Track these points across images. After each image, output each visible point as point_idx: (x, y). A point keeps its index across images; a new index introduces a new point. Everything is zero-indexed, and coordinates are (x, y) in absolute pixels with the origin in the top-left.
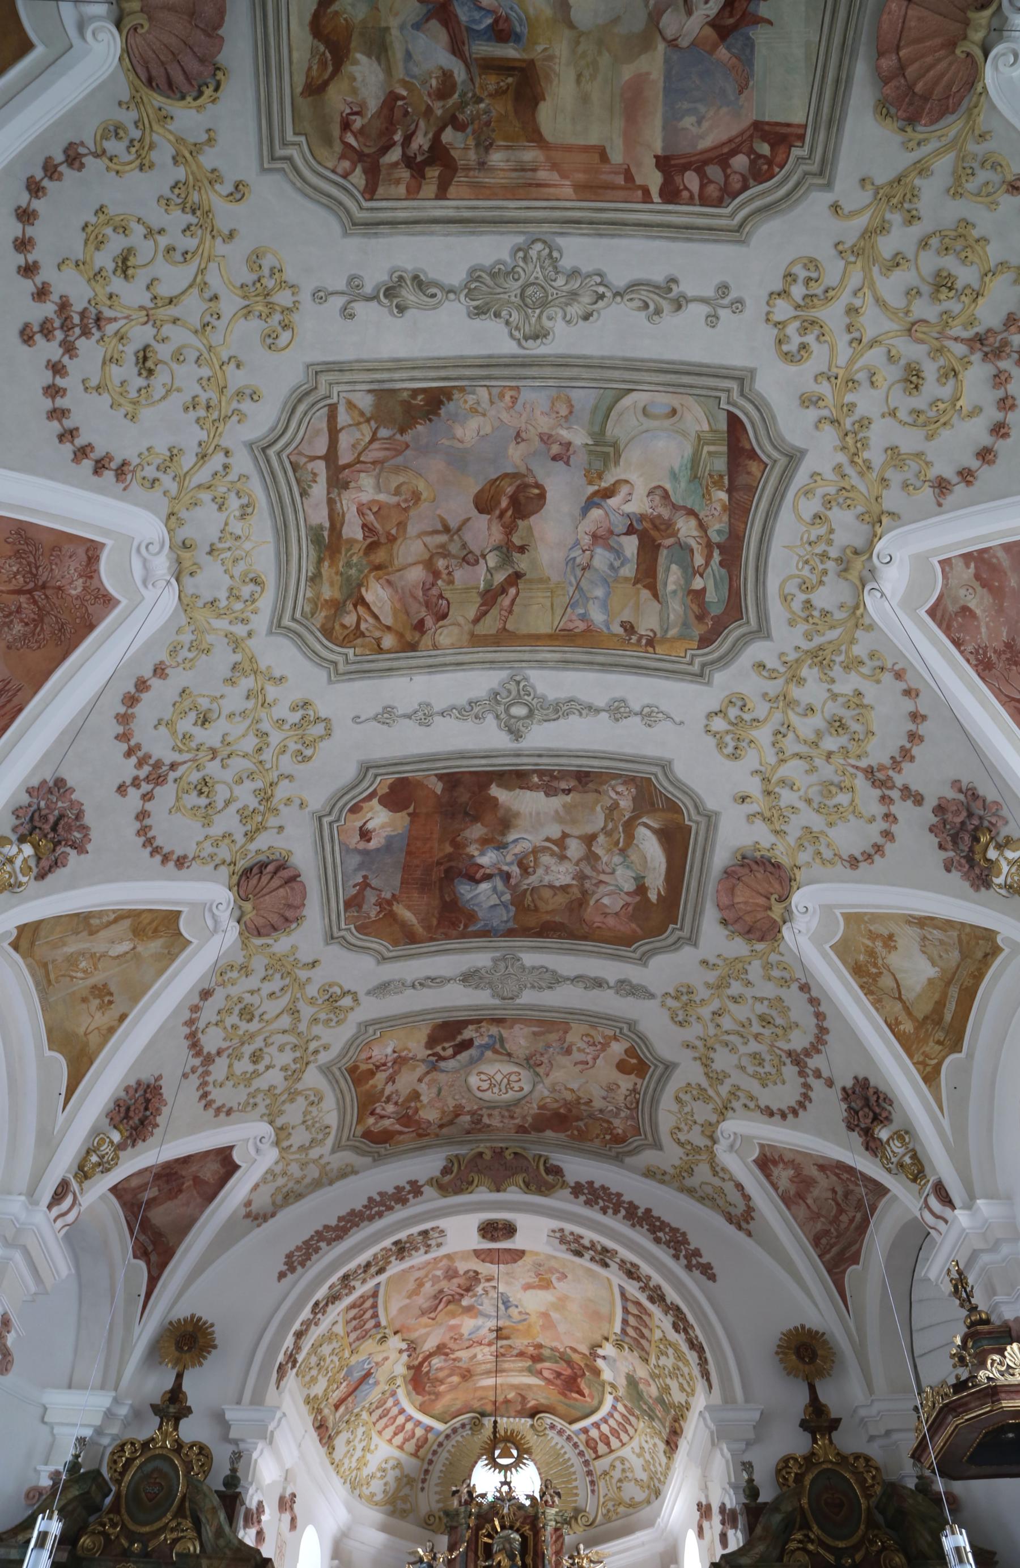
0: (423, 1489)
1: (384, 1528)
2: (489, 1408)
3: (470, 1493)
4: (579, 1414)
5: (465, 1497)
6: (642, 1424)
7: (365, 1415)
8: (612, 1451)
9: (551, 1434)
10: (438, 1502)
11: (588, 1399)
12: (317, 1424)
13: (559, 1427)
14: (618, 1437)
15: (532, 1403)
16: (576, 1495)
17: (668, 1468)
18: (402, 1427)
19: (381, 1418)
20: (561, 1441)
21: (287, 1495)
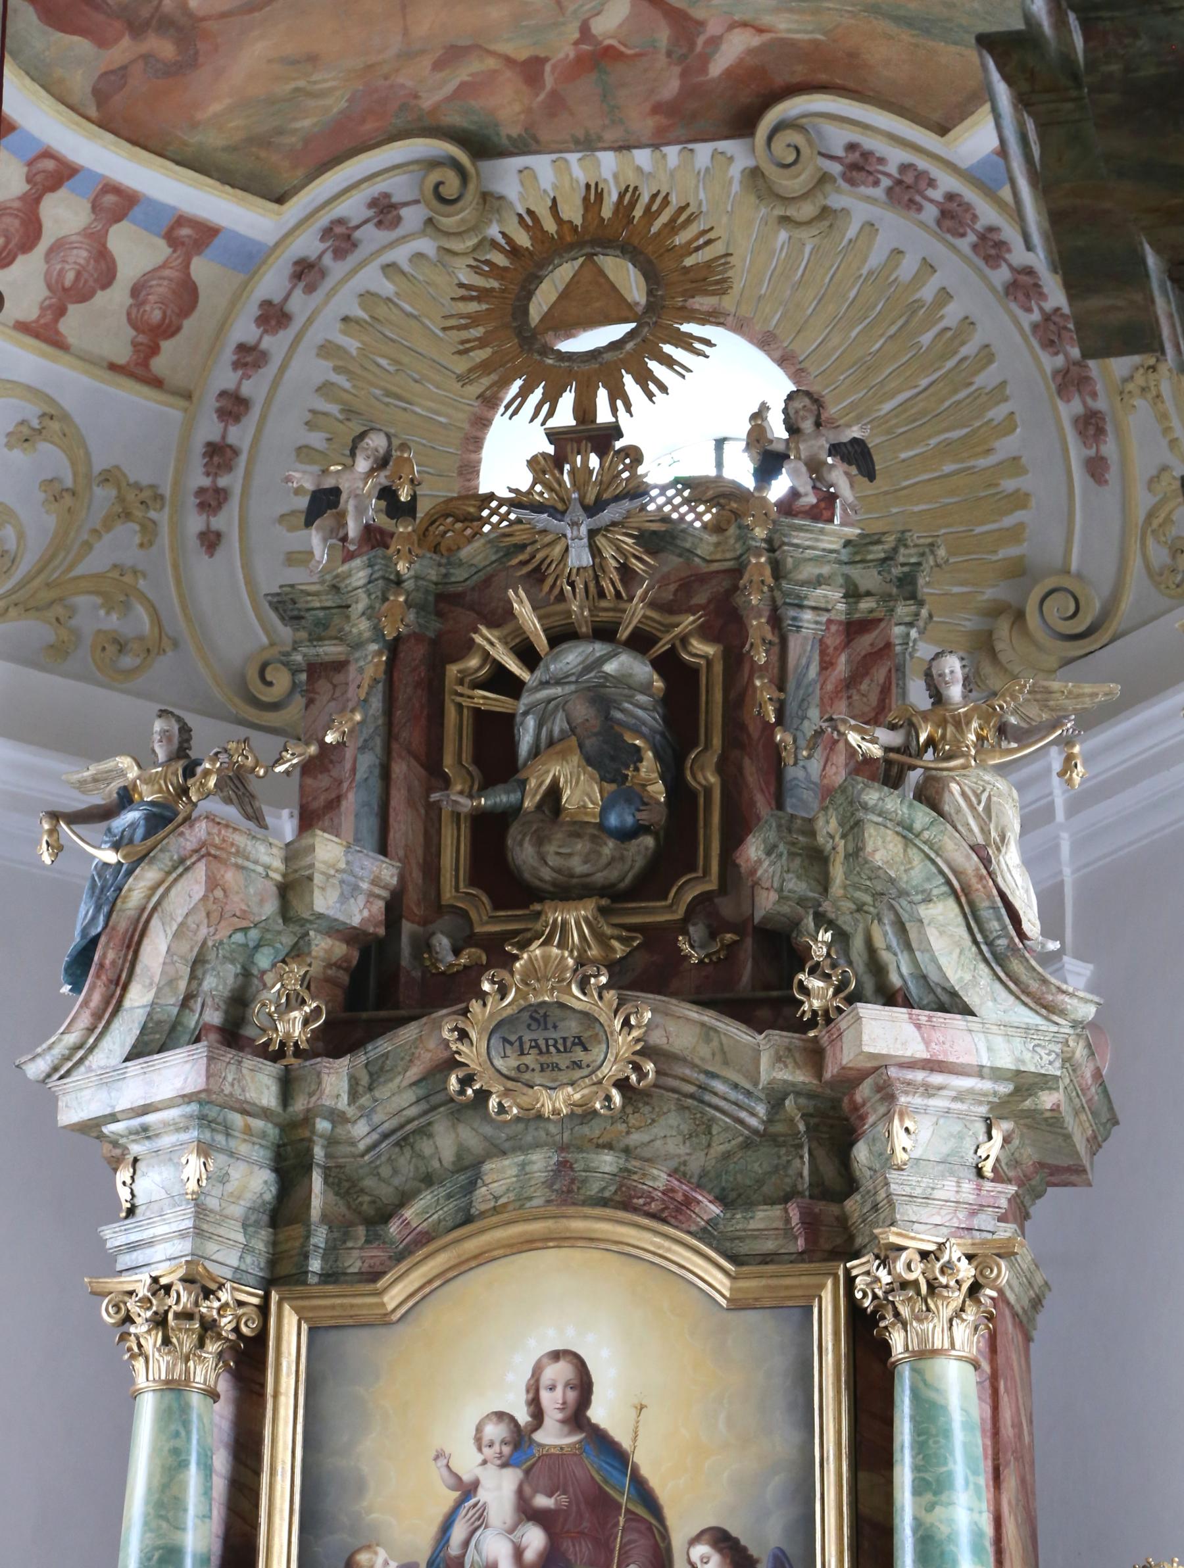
0: (211, 541)
13: (896, 157)
16: (1019, 500)
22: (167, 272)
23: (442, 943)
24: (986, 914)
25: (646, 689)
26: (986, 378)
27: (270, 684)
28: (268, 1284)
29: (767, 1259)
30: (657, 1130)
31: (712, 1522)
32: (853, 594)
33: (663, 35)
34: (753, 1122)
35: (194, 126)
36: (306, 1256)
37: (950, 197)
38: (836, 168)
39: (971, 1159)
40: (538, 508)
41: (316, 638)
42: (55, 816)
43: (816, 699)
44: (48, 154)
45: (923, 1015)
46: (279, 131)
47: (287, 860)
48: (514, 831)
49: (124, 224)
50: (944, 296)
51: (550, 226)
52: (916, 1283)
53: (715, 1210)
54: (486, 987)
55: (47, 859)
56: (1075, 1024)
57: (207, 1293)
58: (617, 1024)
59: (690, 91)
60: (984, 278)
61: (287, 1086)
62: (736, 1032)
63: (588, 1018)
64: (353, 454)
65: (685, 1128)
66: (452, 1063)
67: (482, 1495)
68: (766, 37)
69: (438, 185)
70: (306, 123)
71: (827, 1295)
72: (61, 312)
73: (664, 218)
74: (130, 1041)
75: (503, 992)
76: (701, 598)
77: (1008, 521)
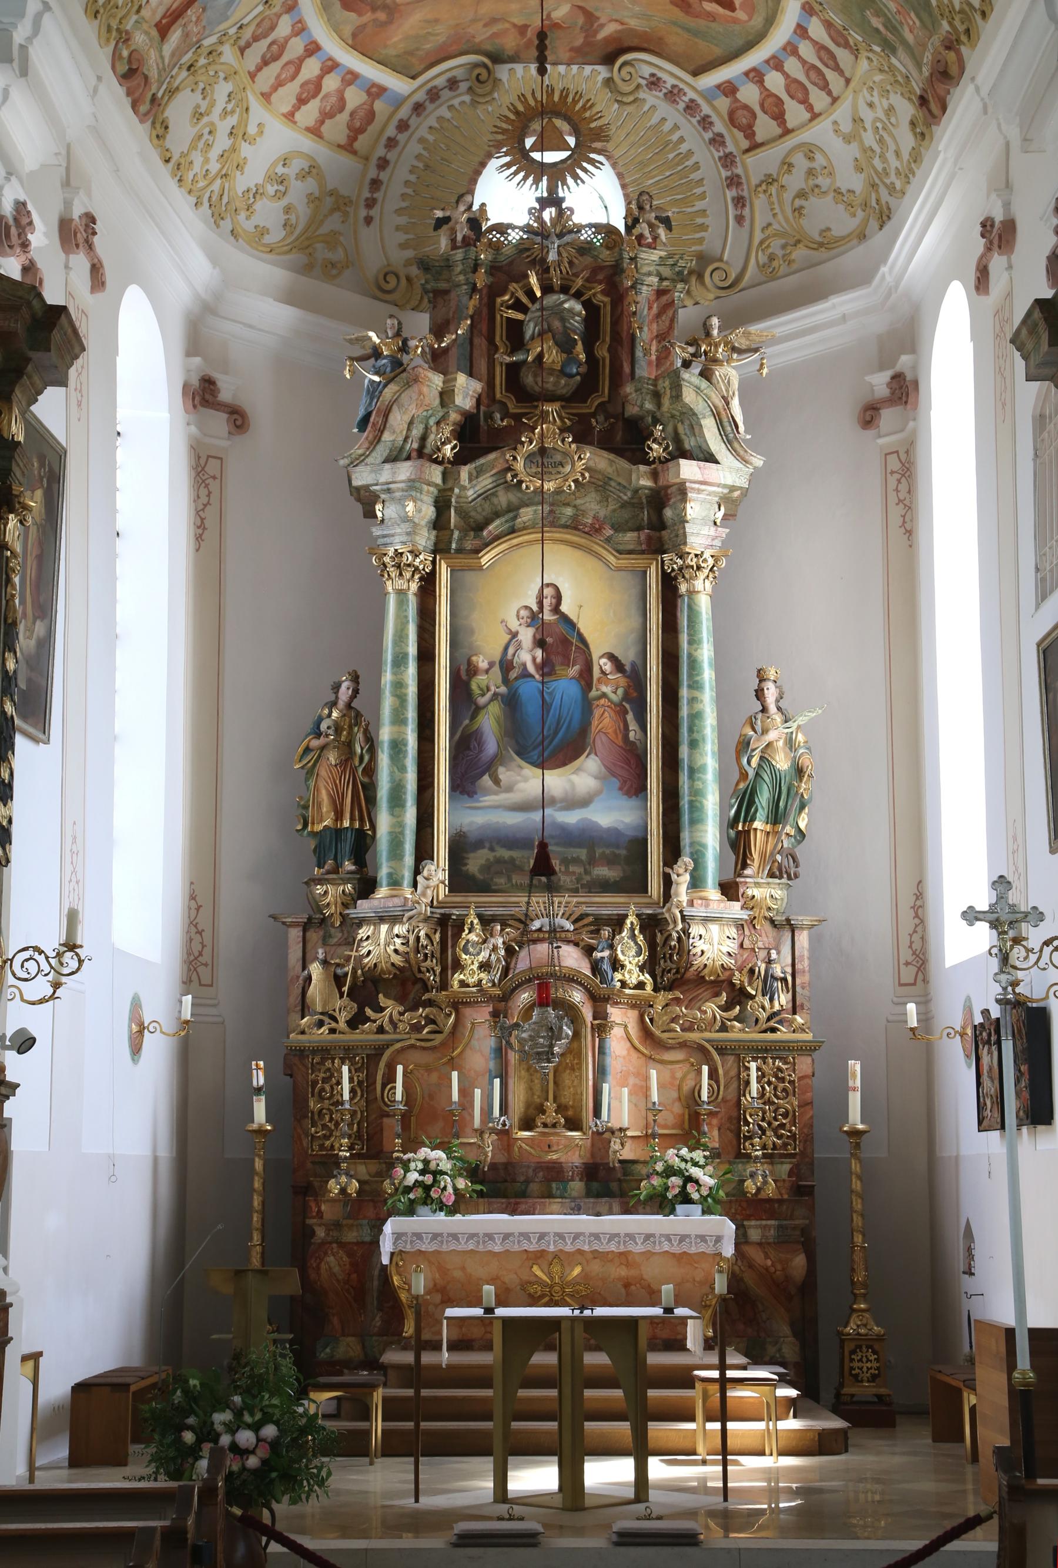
0: (368, 220)
1: (290, 298)
2: (510, 43)
3: (475, 223)
4: (718, 51)
5: (463, 231)
6: (864, 65)
7: (229, 54)
8: (787, 132)
9: (651, 98)
10: (403, 246)
11: (740, 14)
12: (123, 68)
13: (670, 81)
14: (805, 101)
15: (610, 29)
16: (703, 227)
17: (916, 157)
18: (315, 87)
19: (265, 62)
20: (671, 114)
21: (77, 212)
22: (365, 107)
23: (498, 416)
24: (726, 424)
25: (579, 314)
26: (695, 176)
27: (388, 282)
28: (435, 552)
29: (630, 552)
30: (587, 499)
31: (607, 651)
32: (662, 279)
33: (581, 20)
34: (625, 498)
35: (385, 46)
36: (451, 543)
37: (692, 101)
38: (644, 82)
39: (713, 518)
40: (536, 234)
41: (437, 280)
42: (352, 359)
43: (646, 323)
44: (331, 59)
45: (702, 464)
46: (418, 49)
47: (444, 382)
48: (524, 369)
49: (352, 87)
50: (682, 140)
51: (532, 103)
52: (692, 567)
53: (611, 532)
54: (523, 439)
55: (348, 376)
56: (755, 468)
57: (417, 556)
58: (576, 458)
59: (587, 43)
60: (701, 136)
61: (445, 475)
62: (623, 463)
63: (565, 454)
64: (457, 202)
65: (598, 499)
66: (509, 469)
67: (520, 637)
68: (624, 27)
69: (479, 75)
70: (428, 46)
71: (653, 568)
72: (322, 122)
73: (580, 104)
74: (385, 454)
75: (531, 442)
76: (600, 277)
77: (698, 236)
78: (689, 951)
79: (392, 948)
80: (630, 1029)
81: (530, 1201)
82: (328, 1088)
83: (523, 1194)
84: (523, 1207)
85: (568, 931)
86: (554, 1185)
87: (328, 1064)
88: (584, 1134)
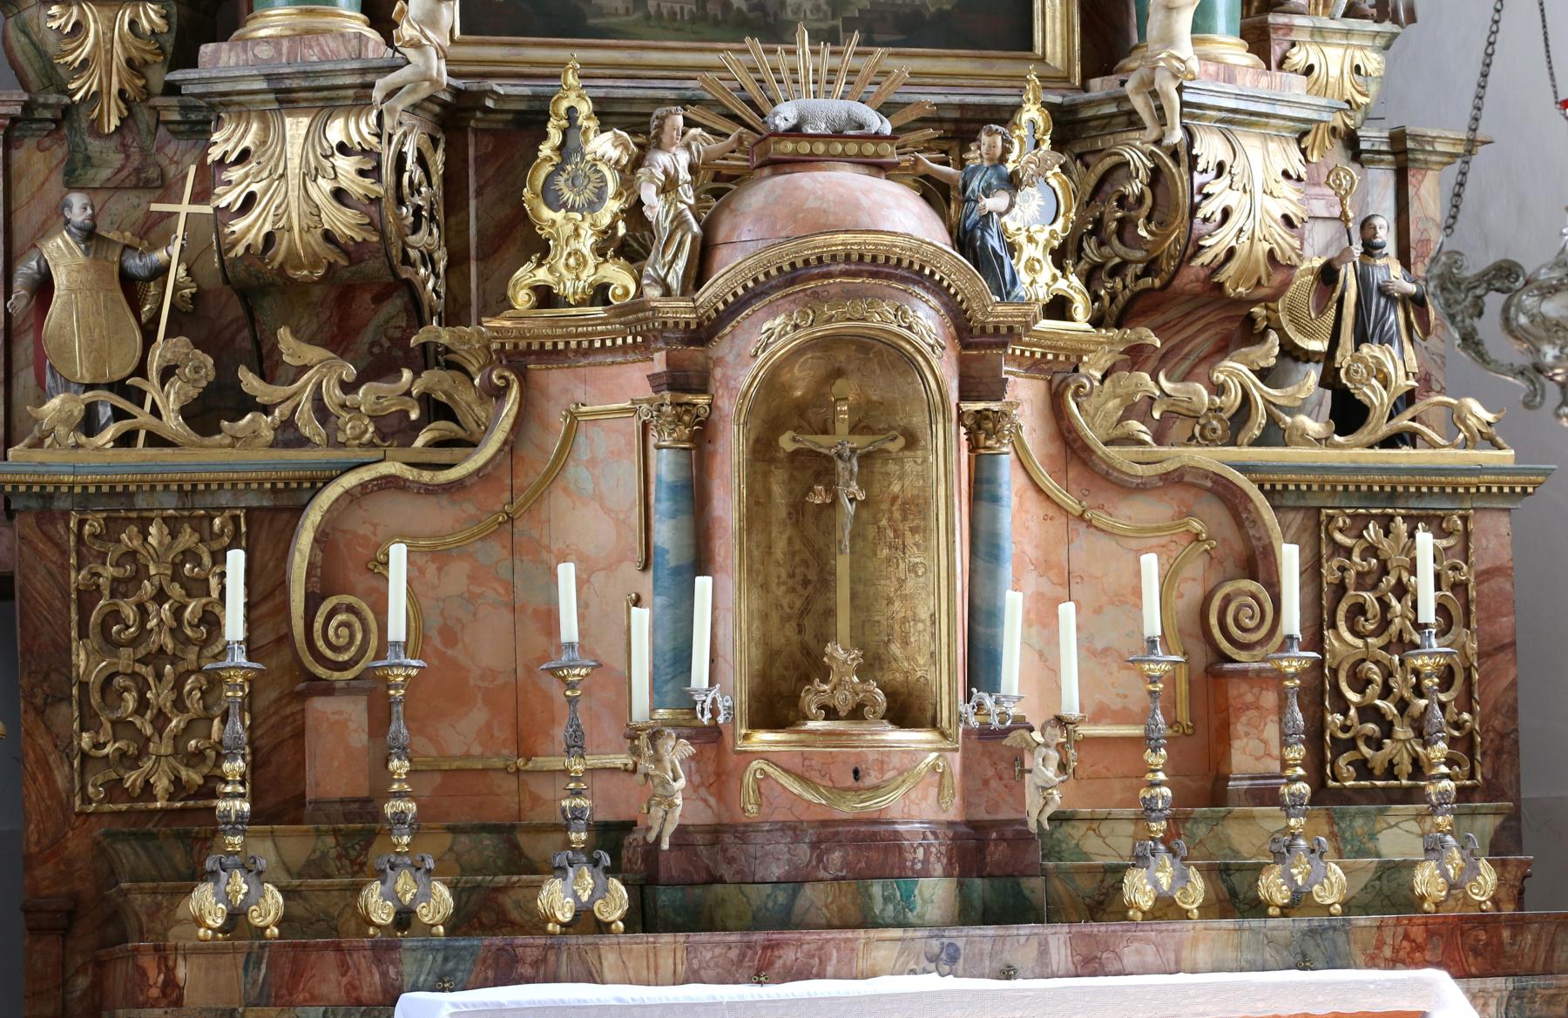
78: (1194, 209)
79: (326, 185)
80: (1025, 435)
81: (812, 937)
82: (129, 612)
83: (786, 920)
84: (789, 956)
85: (877, 137)
86: (877, 889)
87: (129, 538)
88: (943, 735)
